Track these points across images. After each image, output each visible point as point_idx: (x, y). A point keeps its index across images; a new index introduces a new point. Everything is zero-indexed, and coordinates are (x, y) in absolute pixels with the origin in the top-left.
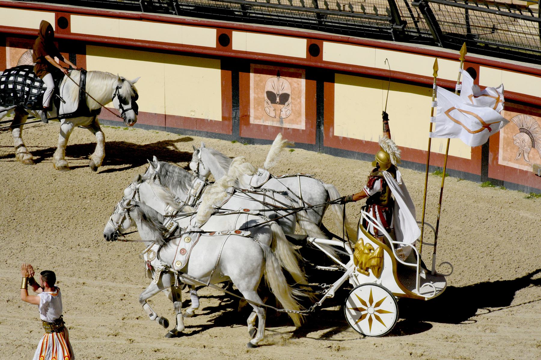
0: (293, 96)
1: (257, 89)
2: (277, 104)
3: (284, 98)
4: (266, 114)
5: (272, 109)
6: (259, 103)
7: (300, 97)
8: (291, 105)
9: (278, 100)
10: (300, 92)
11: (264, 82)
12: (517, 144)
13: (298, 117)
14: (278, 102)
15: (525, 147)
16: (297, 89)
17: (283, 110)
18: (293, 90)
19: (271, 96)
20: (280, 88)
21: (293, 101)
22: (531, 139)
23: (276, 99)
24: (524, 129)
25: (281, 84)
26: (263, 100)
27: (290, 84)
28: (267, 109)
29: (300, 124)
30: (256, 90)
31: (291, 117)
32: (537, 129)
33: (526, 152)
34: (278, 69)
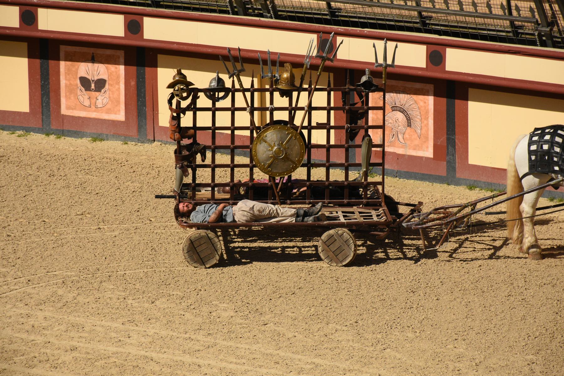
0: (110, 82)
1: (69, 74)
2: (91, 91)
3: (100, 84)
4: (79, 103)
5: (87, 97)
6: (71, 90)
7: (118, 83)
8: (108, 92)
9: (93, 86)
10: (118, 77)
11: (76, 67)
12: (390, 124)
13: (117, 106)
14: (93, 89)
15: (400, 128)
16: (114, 74)
17: (99, 98)
18: (110, 75)
19: (85, 82)
20: (96, 72)
21: (110, 87)
22: (406, 117)
23: (91, 86)
24: (397, 107)
25: (96, 68)
26: (76, 87)
27: (107, 68)
28: (80, 97)
29: (119, 114)
30: (68, 76)
31: (108, 106)
32: (413, 106)
33: (401, 133)
34: (91, 50)
